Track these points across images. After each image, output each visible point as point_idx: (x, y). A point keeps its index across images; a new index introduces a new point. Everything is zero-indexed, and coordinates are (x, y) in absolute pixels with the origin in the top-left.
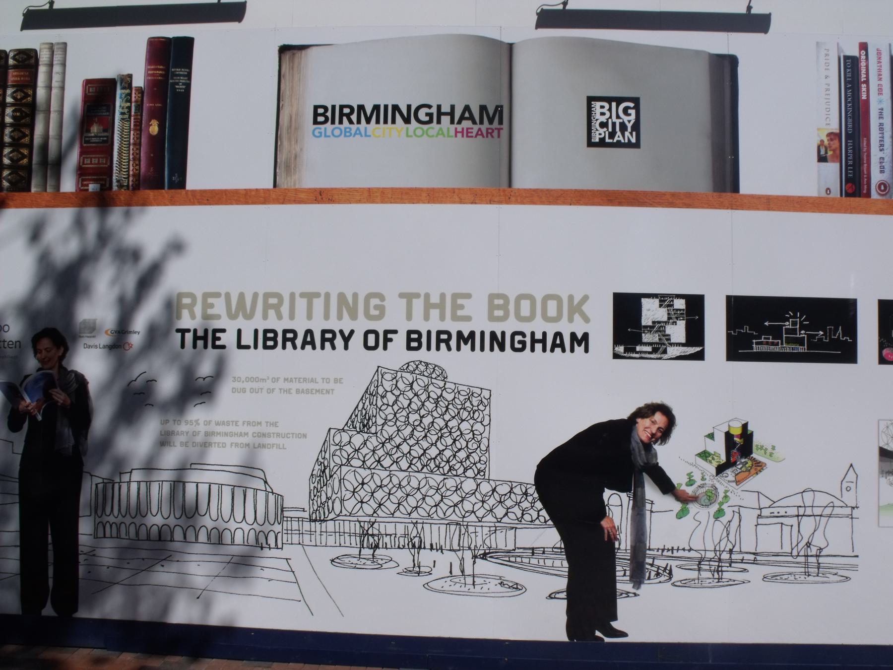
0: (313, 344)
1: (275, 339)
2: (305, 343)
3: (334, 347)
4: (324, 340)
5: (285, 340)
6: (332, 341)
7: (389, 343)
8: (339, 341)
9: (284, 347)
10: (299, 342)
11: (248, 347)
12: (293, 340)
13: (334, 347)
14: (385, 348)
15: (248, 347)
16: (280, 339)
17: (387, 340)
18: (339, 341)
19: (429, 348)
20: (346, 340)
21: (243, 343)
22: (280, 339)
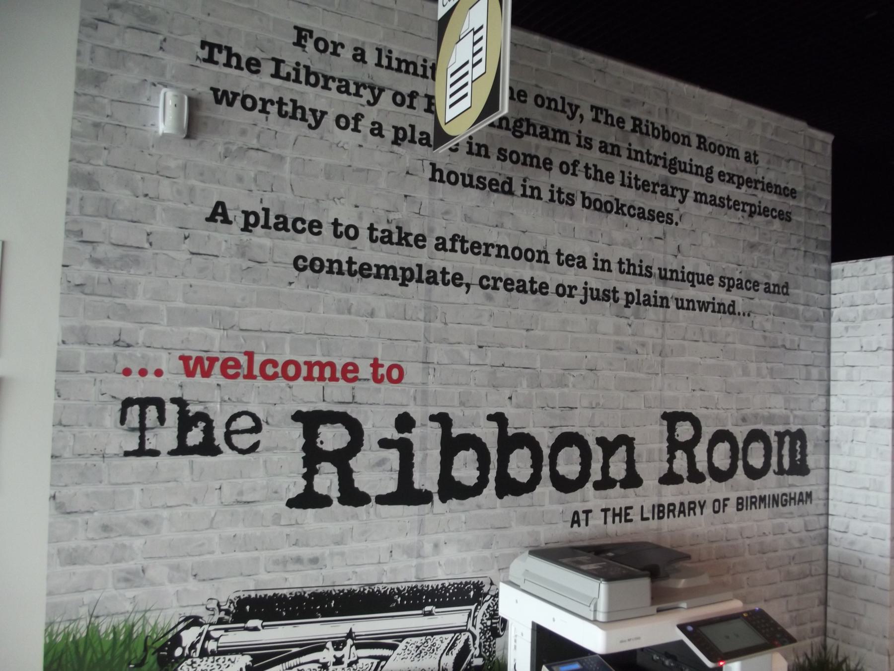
0: (684, 512)
1: (663, 511)
2: (680, 512)
3: (695, 514)
4: (690, 509)
5: (669, 511)
6: (694, 509)
7: (726, 508)
8: (698, 510)
9: (668, 517)
10: (677, 513)
11: (647, 519)
12: (673, 511)
13: (695, 514)
14: (724, 511)
15: (647, 519)
16: (666, 511)
17: (725, 505)
18: (698, 510)
19: (747, 509)
20: (702, 507)
21: (645, 516)
22: (666, 511)
